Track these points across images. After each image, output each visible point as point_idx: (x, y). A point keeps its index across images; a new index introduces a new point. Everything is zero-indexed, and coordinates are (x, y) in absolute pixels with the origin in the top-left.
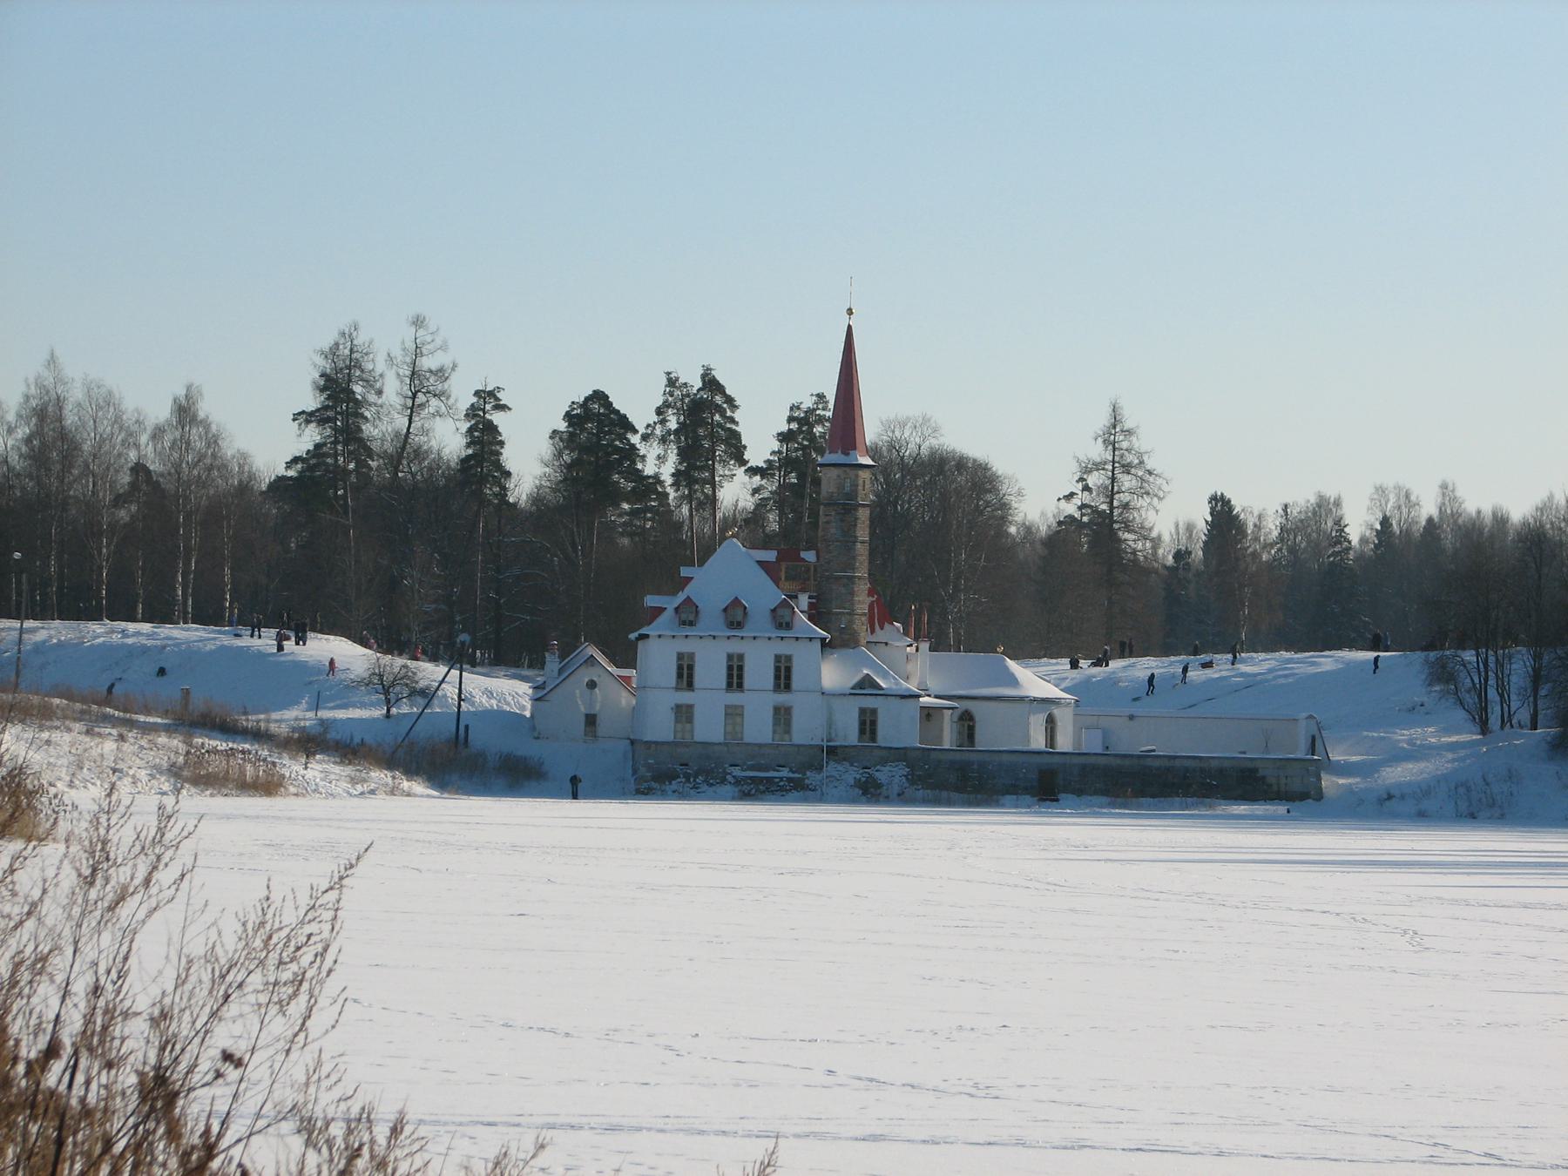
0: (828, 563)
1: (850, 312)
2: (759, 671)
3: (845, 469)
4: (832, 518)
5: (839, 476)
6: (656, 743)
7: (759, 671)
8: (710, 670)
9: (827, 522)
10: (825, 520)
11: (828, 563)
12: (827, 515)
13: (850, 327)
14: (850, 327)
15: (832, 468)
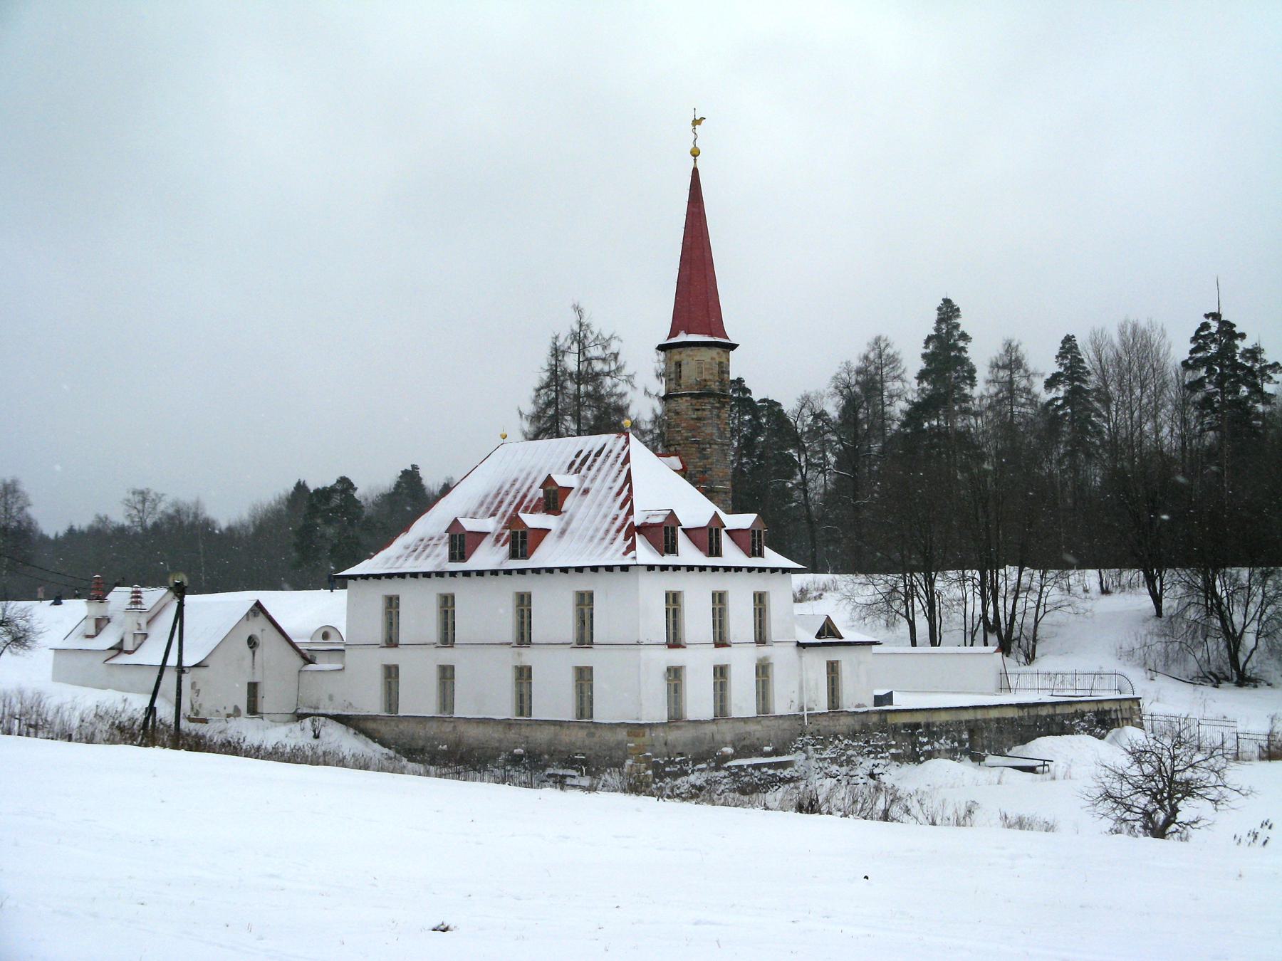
0: (704, 472)
1: (695, 153)
2: (741, 621)
3: (718, 350)
4: (707, 413)
5: (712, 359)
6: (651, 726)
7: (741, 621)
8: (697, 621)
9: (699, 419)
10: (694, 416)
11: (704, 472)
12: (698, 410)
13: (695, 171)
14: (695, 172)
15: (703, 349)
